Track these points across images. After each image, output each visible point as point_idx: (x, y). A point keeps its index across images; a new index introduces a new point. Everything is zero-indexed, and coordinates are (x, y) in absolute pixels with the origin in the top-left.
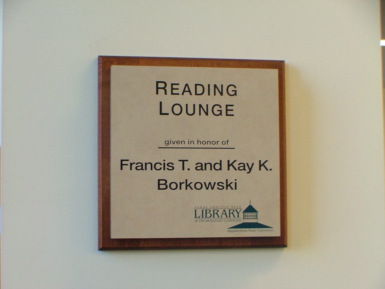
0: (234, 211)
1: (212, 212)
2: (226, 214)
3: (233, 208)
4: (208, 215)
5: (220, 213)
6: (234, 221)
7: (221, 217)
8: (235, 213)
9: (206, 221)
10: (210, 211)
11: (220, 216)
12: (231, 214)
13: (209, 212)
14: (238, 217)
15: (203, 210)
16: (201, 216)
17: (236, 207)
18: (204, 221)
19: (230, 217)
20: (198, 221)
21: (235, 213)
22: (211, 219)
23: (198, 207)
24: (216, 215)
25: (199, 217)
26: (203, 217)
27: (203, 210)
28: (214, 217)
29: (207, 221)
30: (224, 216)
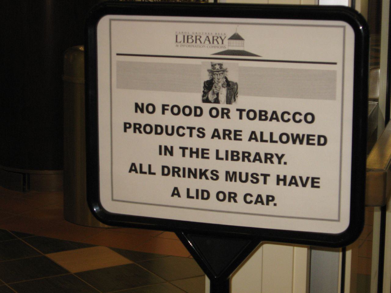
0: (218, 38)
1: (194, 38)
2: (209, 41)
3: (217, 34)
4: (190, 40)
5: (203, 40)
6: (218, 47)
7: (204, 43)
8: (219, 40)
9: (187, 46)
10: (192, 37)
11: (203, 42)
12: (215, 42)
13: (191, 38)
14: (223, 43)
15: (184, 36)
16: (183, 41)
17: (220, 34)
18: (185, 46)
19: (213, 43)
20: (179, 46)
21: (219, 40)
22: (193, 45)
23: (180, 33)
24: (198, 41)
25: (180, 42)
26: (184, 42)
27: (184, 36)
28: (196, 42)
29: (189, 46)
30: (207, 42)
